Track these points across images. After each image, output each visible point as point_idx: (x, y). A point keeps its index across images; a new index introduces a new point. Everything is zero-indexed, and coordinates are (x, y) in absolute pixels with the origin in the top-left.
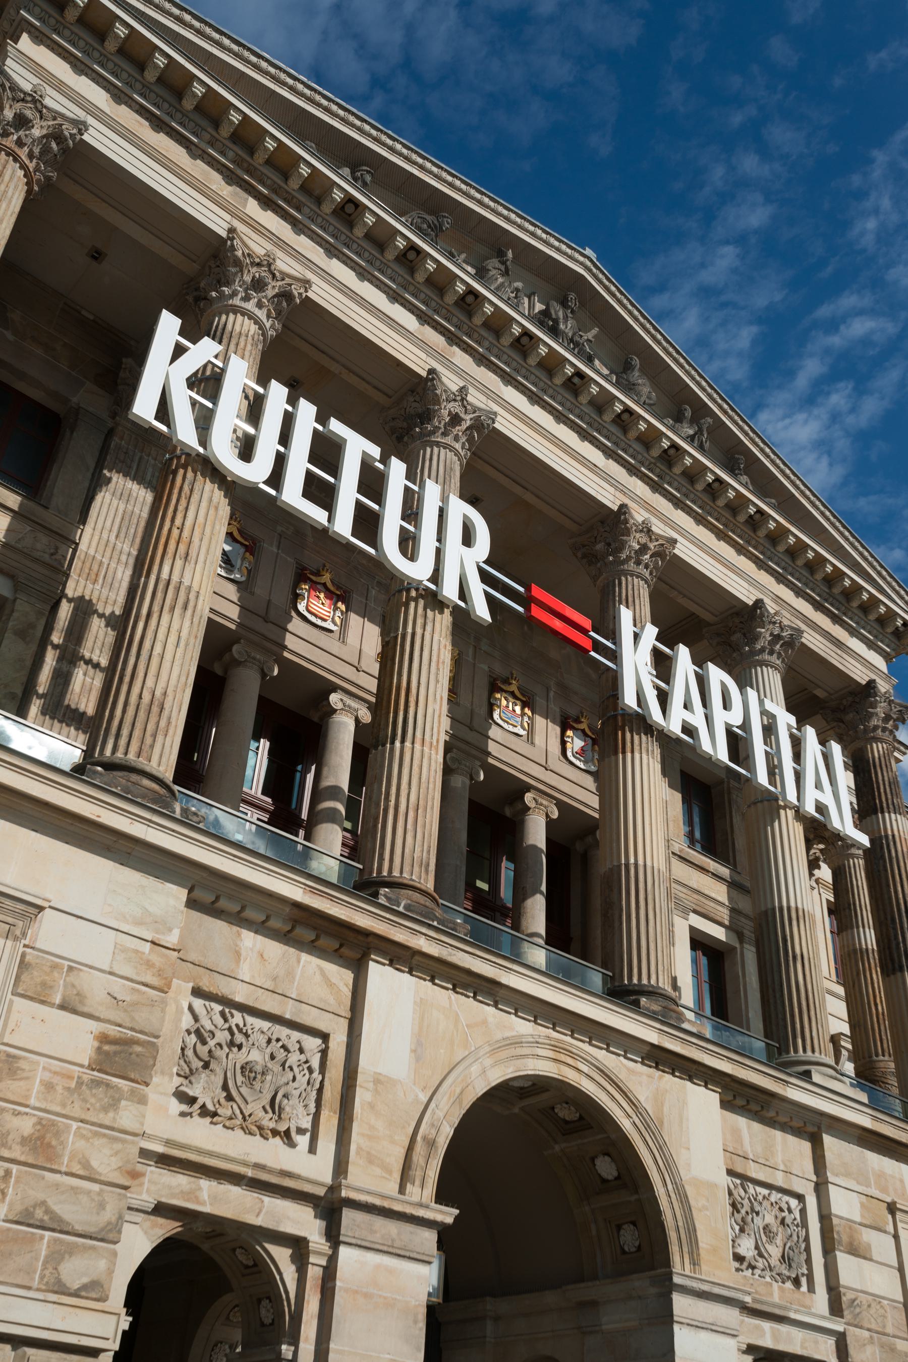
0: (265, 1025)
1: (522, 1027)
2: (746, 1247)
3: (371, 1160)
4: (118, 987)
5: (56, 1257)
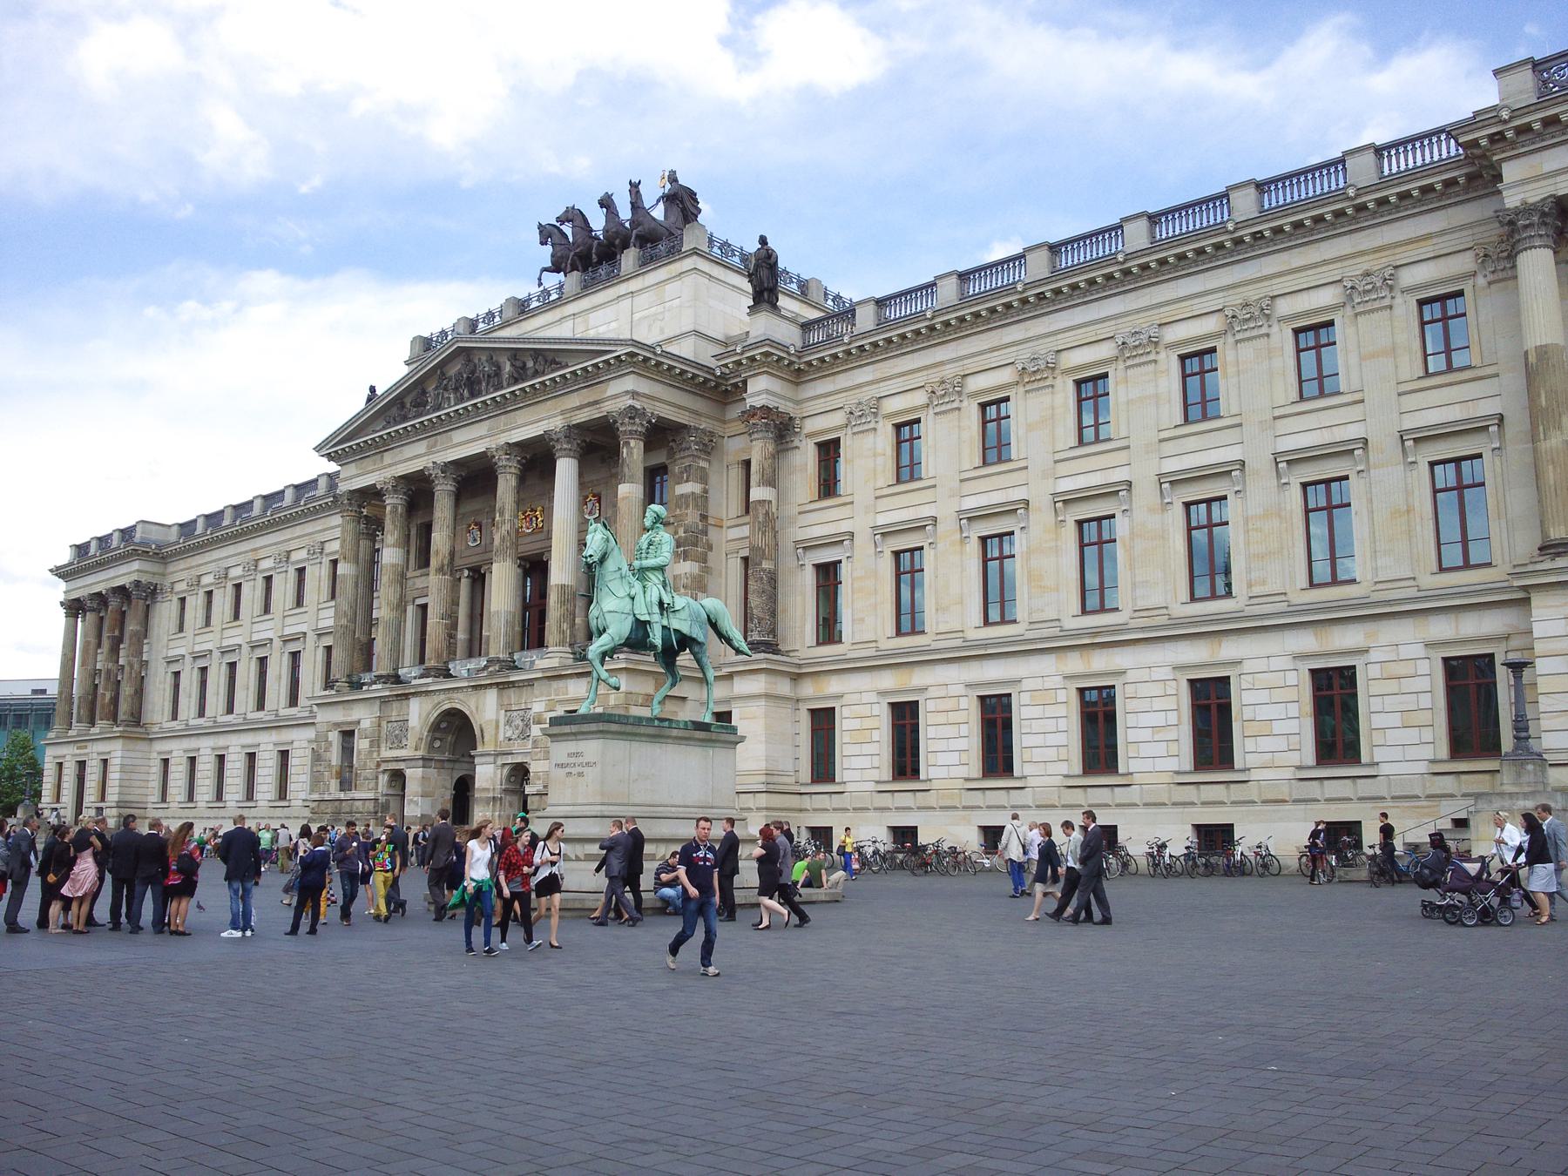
1: (442, 697)
2: (509, 734)
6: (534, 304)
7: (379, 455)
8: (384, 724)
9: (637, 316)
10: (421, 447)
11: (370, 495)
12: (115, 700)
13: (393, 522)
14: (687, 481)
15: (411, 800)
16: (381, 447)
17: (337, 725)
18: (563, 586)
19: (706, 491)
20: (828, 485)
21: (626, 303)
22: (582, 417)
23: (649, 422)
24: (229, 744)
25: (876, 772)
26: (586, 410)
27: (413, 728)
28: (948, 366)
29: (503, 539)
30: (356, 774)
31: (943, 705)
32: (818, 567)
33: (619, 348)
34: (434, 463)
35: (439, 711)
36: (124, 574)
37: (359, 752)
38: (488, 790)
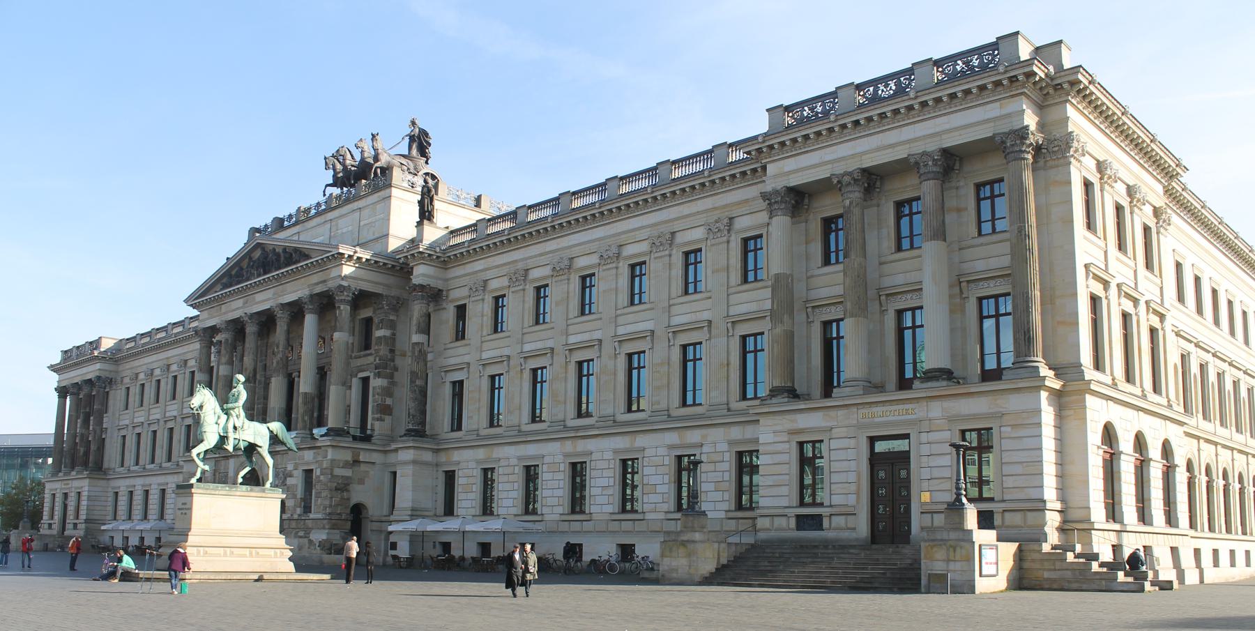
6: (313, 212)
7: (219, 307)
8: (217, 474)
9: (362, 223)
10: (240, 303)
11: (213, 330)
12: (87, 453)
13: (225, 349)
14: (382, 328)
16: (220, 300)
18: (306, 393)
19: (394, 334)
20: (460, 335)
21: (357, 214)
22: (318, 289)
23: (354, 294)
24: (151, 482)
25: (473, 510)
27: (231, 477)
29: (278, 363)
32: (454, 383)
33: (333, 250)
34: (246, 313)
36: (90, 371)
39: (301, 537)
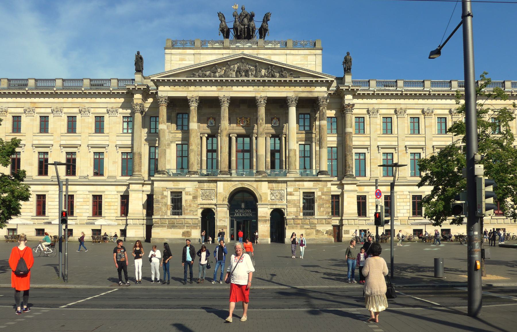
0: (209, 191)
1: (237, 183)
2: (273, 198)
3: (219, 200)
4: (193, 192)
5: (193, 213)
15: (221, 220)
17: (171, 189)
26: (305, 93)
28: (402, 105)
30: (184, 208)
31: (402, 197)
35: (235, 188)
37: (186, 201)
38: (265, 217)
39: (308, 229)
